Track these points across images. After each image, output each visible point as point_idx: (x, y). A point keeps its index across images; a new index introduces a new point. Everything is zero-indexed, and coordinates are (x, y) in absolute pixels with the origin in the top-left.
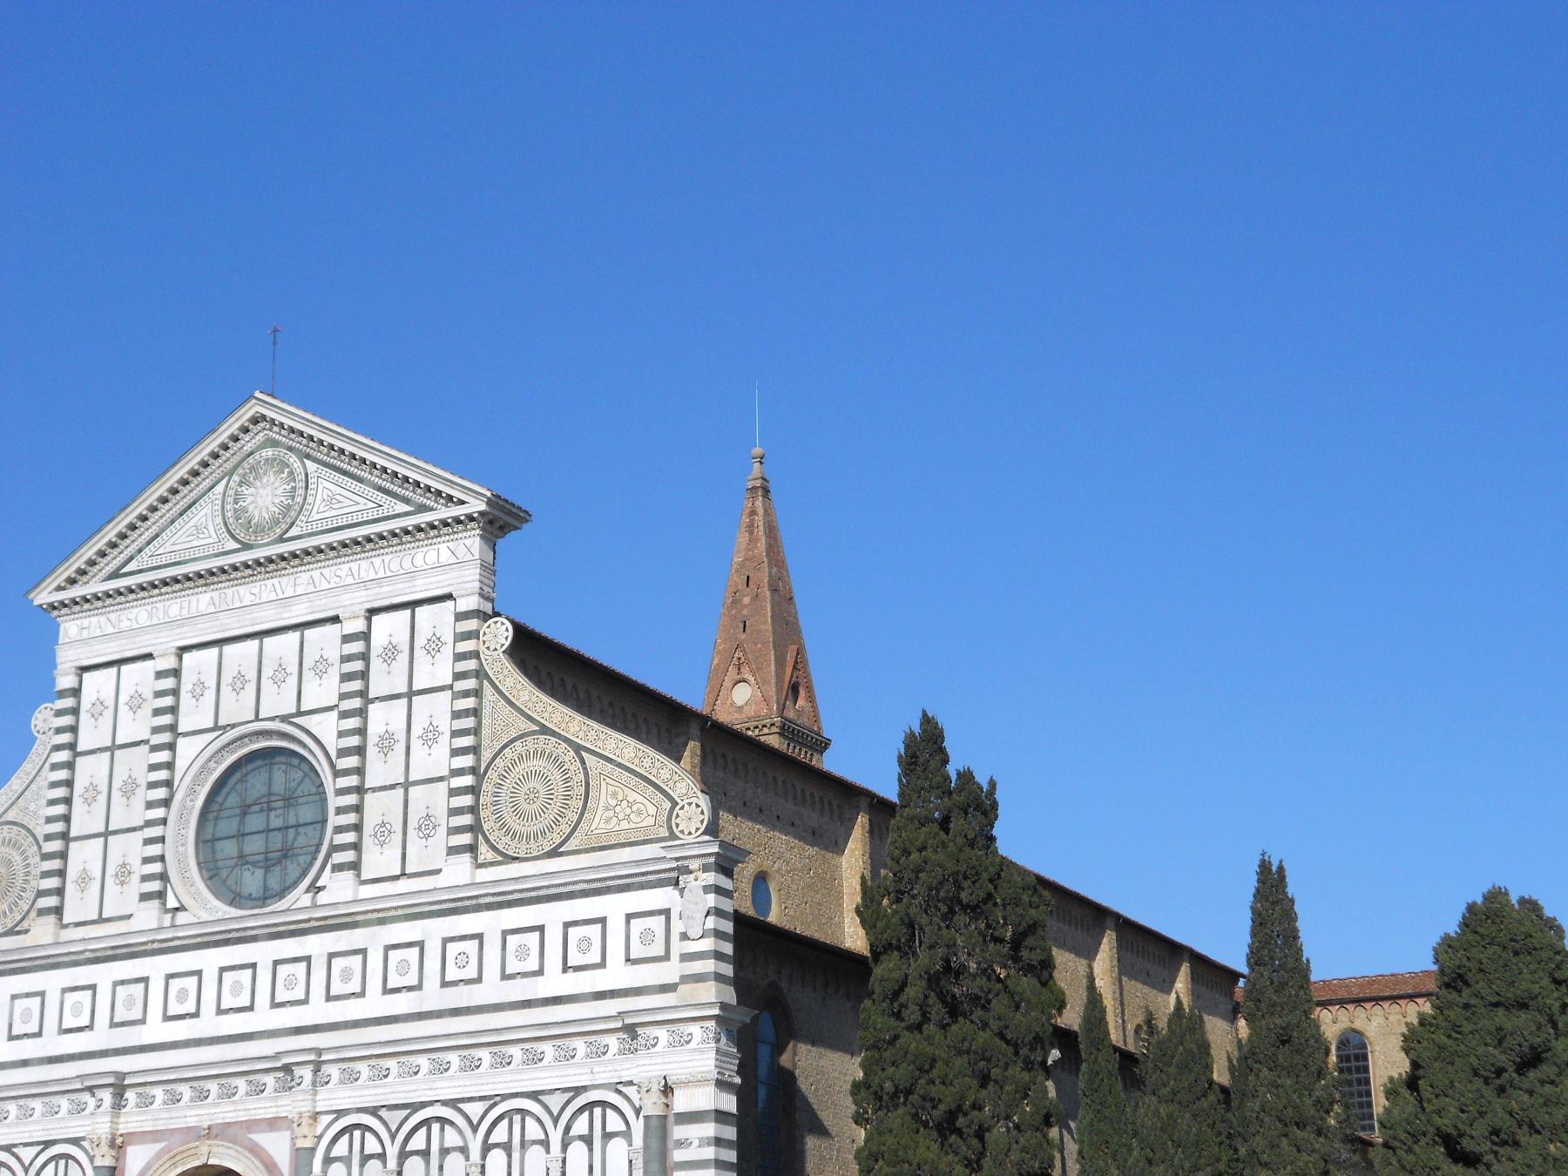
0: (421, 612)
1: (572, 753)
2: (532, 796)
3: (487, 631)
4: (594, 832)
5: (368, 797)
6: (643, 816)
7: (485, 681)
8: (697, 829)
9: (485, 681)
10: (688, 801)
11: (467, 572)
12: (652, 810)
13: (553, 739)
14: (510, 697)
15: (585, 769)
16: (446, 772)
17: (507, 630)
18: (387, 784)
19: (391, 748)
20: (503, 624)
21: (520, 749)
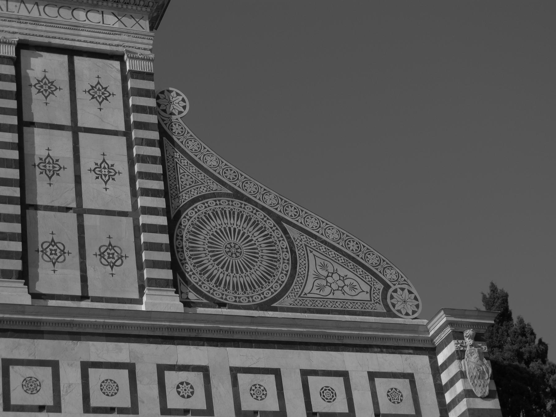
0: (80, 62)
1: (272, 222)
2: (233, 250)
3: (161, 95)
4: (309, 295)
5: (30, 213)
6: (357, 291)
7: (164, 138)
8: (414, 312)
9: (164, 138)
10: (400, 286)
11: (140, 40)
12: (366, 288)
13: (249, 206)
14: (196, 159)
15: (289, 238)
16: (128, 208)
17: (183, 100)
18: (56, 204)
19: (55, 172)
20: (178, 94)
21: (213, 206)
